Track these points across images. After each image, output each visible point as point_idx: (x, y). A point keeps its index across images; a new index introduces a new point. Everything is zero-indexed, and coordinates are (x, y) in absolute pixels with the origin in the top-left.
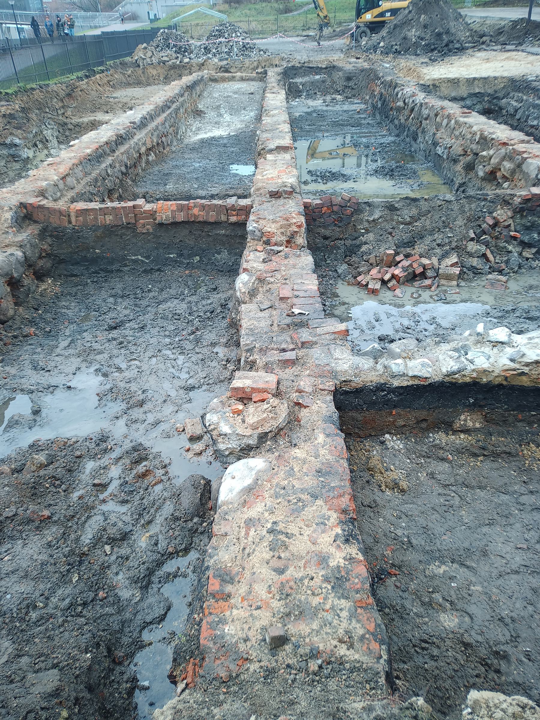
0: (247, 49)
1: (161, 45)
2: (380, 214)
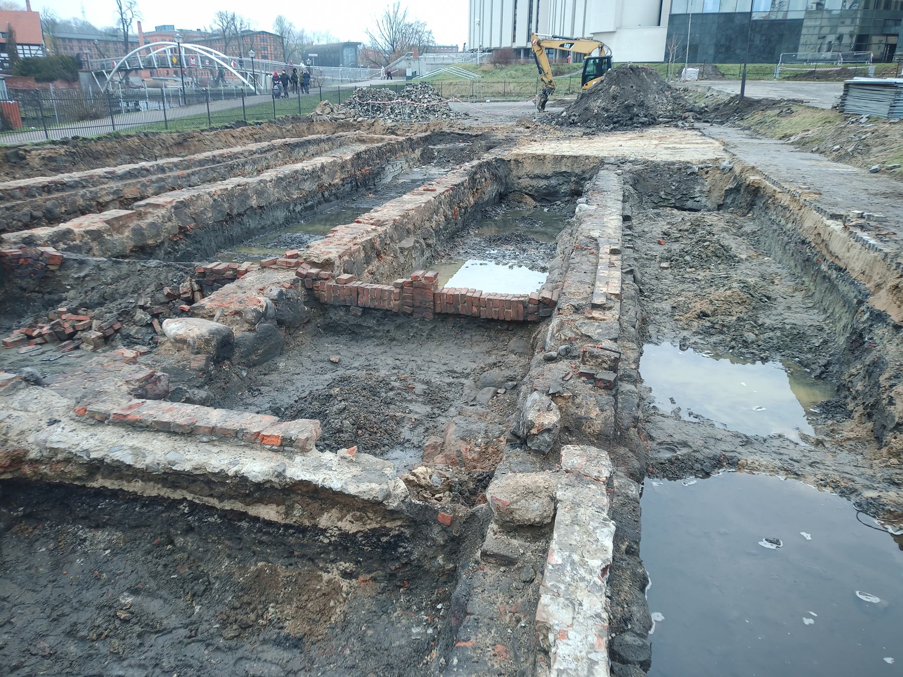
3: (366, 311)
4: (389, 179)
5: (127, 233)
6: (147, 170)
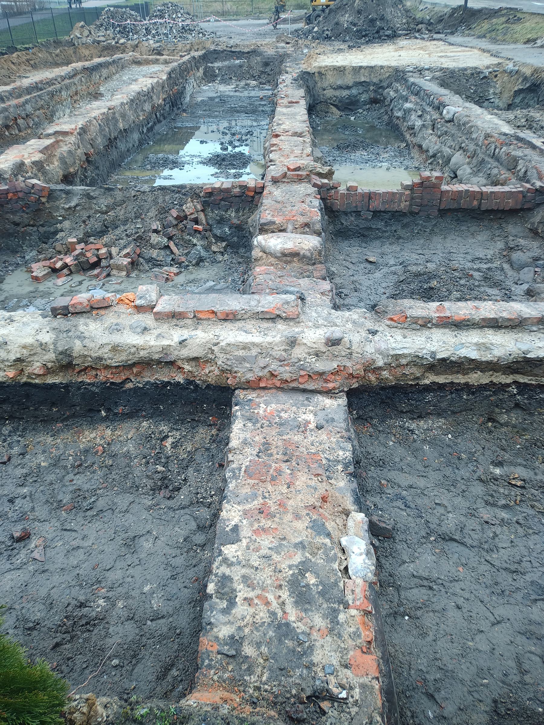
0: (186, 31)
1: (105, 24)
2: (77, 202)
3: (377, 214)
4: (188, 99)
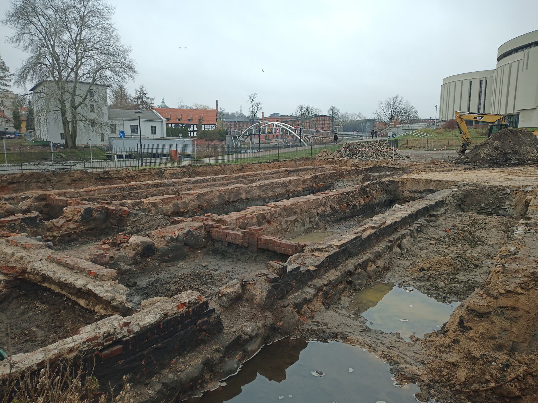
3: (230, 244)
5: (171, 205)
6: (207, 180)
